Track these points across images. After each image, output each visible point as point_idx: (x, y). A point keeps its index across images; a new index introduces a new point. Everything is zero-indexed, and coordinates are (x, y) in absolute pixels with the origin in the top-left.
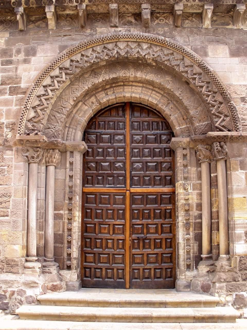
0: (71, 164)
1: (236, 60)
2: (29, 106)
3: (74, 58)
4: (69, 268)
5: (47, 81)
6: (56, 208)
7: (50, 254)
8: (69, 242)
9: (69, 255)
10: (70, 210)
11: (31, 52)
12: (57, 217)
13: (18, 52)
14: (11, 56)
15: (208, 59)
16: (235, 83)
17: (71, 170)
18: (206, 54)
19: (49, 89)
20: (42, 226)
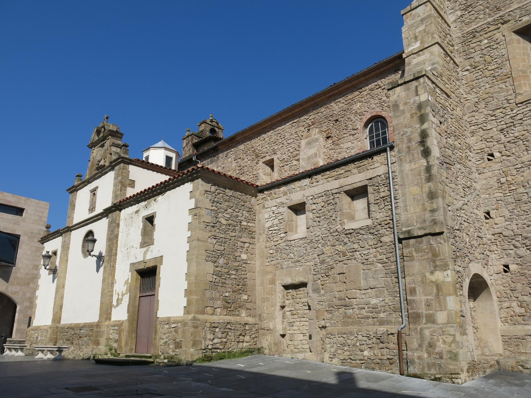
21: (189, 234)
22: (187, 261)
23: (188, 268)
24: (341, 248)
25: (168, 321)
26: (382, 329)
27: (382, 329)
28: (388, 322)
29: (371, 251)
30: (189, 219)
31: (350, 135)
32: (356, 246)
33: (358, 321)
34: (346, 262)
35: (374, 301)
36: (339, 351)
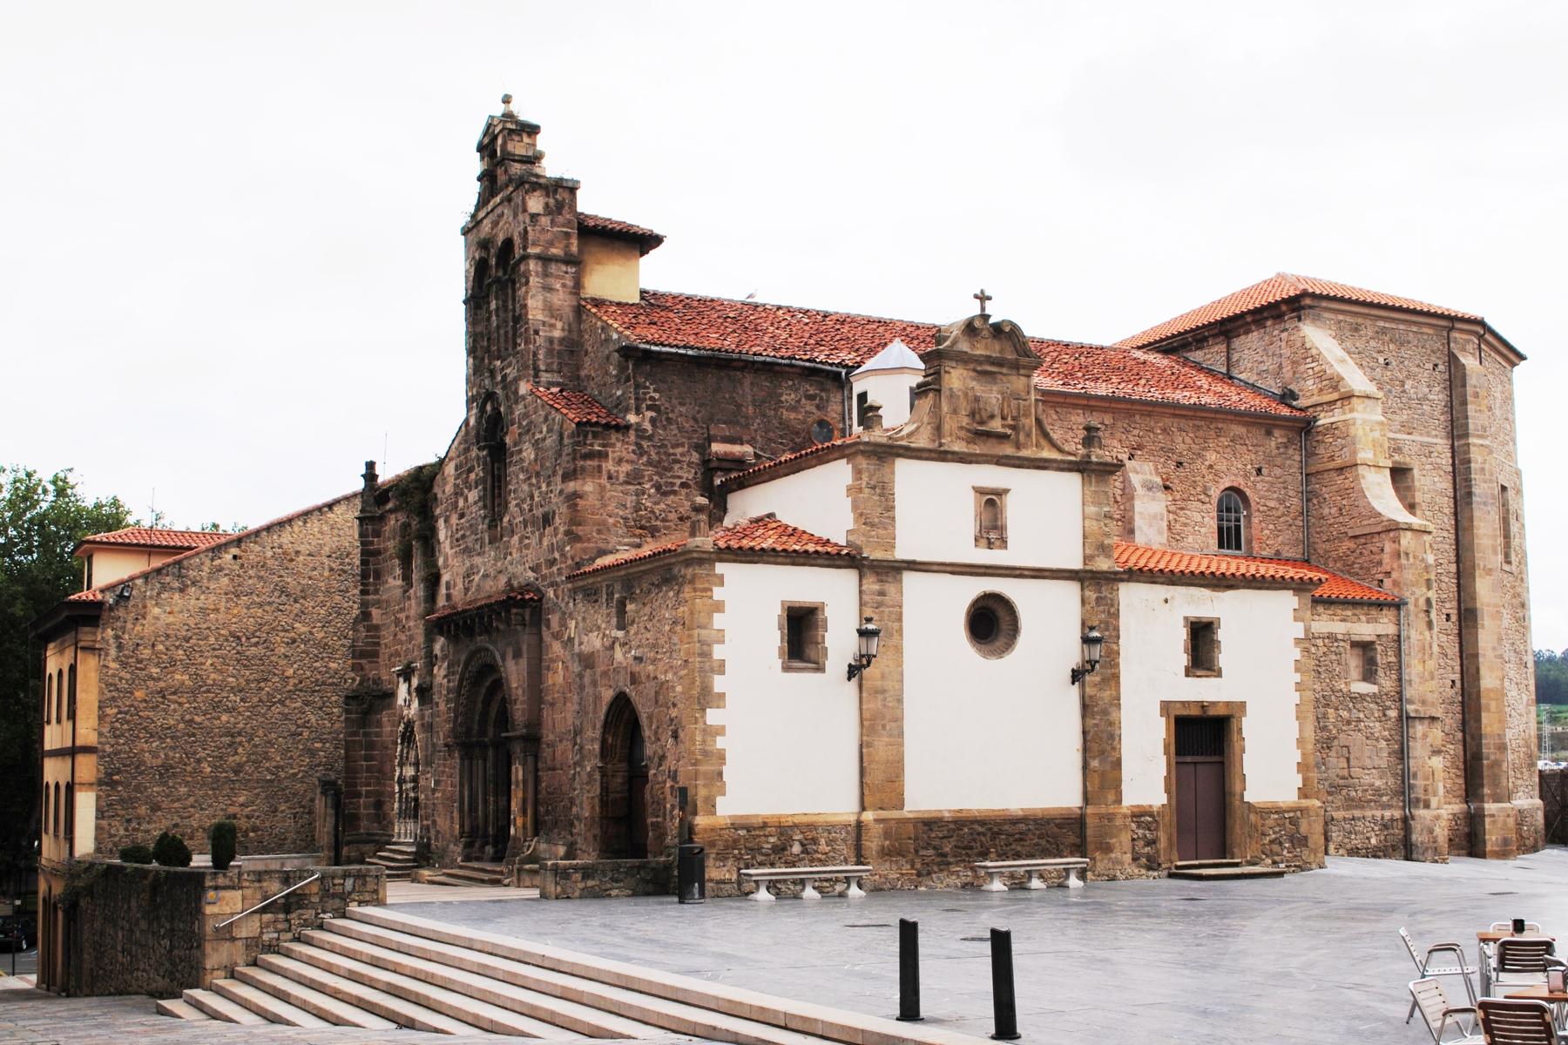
7: (480, 832)
21: (1297, 677)
22: (1298, 718)
23: (1301, 731)
24: (1345, 714)
25: (1264, 812)
26: (1387, 814)
27: (1387, 814)
28: (1390, 807)
29: (1377, 724)
30: (1297, 653)
31: (1199, 500)
32: (1361, 715)
33: (1360, 804)
34: (1350, 733)
35: (1378, 783)
36: (1346, 840)
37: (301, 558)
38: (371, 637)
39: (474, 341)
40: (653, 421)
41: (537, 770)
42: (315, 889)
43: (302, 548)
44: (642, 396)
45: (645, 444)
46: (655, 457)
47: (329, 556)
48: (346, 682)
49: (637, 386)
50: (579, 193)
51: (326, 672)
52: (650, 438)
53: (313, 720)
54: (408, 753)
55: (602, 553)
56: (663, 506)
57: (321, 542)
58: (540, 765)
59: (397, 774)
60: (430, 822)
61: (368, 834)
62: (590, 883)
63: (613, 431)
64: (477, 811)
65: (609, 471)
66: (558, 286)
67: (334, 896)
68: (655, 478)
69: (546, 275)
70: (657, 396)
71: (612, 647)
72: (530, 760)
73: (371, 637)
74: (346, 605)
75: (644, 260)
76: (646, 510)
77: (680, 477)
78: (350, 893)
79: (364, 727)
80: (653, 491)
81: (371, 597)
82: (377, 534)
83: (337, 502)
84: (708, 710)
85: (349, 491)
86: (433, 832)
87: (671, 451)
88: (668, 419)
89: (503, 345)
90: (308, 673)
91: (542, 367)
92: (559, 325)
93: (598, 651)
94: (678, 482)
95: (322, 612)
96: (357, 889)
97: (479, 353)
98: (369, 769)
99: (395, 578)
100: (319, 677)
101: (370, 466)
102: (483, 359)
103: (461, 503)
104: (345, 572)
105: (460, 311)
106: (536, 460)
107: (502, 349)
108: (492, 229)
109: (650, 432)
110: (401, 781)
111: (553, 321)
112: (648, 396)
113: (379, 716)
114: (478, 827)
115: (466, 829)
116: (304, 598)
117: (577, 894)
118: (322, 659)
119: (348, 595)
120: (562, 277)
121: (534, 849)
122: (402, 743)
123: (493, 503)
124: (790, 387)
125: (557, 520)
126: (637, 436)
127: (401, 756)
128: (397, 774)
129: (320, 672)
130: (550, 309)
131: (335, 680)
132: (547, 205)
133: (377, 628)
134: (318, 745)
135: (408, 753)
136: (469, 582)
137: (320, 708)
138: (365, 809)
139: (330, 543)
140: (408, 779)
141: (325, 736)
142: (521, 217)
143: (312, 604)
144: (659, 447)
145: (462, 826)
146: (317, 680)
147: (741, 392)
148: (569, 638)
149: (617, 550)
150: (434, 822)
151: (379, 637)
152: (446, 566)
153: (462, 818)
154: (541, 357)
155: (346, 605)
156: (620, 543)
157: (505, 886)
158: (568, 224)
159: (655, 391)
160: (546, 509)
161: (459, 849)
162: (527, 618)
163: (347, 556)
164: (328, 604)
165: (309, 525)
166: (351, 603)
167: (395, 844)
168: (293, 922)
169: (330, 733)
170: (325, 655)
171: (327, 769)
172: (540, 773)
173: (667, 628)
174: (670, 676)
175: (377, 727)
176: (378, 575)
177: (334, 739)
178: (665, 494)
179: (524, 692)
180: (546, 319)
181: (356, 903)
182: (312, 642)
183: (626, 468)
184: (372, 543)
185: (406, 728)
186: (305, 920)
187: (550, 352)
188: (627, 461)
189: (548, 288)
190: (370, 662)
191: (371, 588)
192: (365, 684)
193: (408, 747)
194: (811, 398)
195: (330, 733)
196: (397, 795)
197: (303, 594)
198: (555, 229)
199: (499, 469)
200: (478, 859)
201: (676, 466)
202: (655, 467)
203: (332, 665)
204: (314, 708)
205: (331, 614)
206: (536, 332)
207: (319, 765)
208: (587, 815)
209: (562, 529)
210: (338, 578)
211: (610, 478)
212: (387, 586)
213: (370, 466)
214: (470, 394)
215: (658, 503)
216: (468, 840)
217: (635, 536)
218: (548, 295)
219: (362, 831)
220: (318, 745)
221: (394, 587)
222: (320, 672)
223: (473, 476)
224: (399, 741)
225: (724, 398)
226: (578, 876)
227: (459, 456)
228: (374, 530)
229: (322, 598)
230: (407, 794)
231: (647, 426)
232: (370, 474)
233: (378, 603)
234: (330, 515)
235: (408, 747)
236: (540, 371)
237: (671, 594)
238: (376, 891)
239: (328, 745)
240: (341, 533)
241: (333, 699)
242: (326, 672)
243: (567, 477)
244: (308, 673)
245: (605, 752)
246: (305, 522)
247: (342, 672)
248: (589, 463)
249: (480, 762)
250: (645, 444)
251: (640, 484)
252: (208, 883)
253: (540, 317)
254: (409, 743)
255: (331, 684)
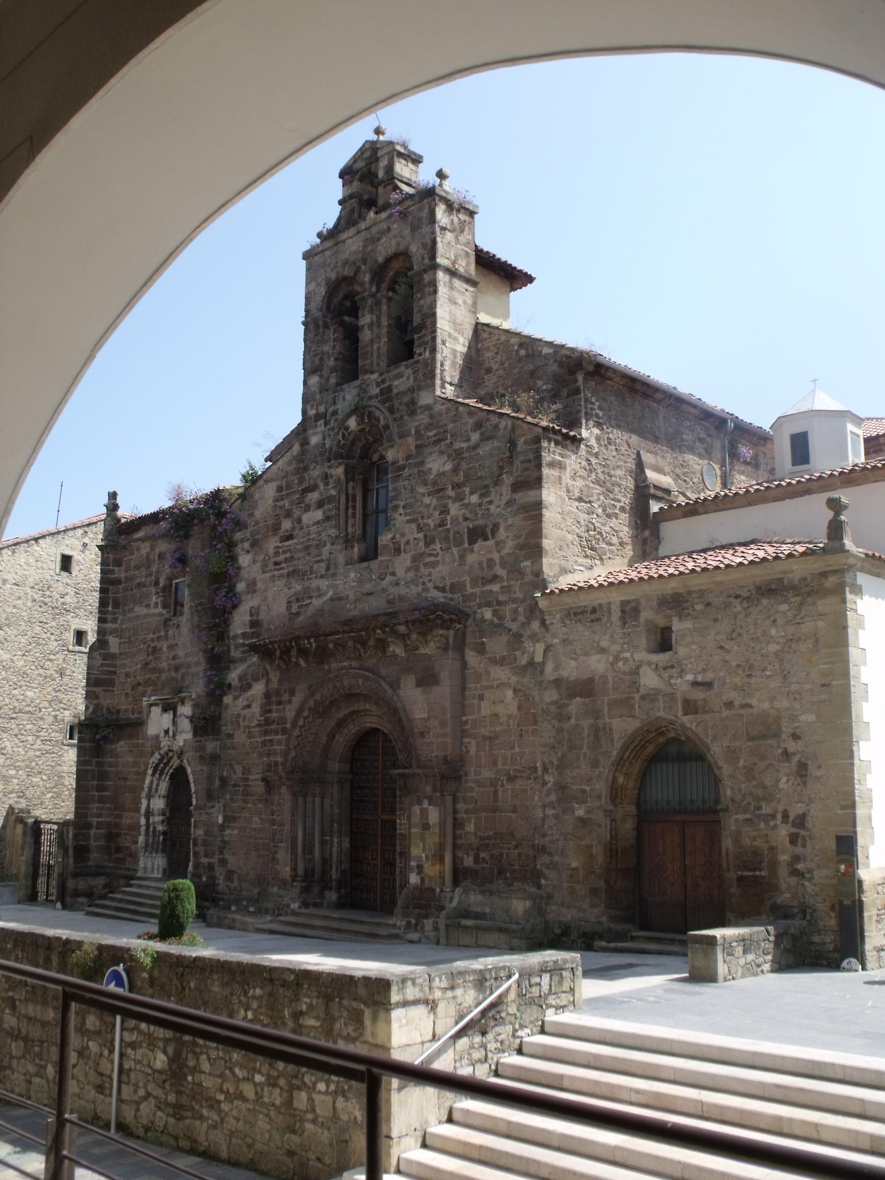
0: (332, 793)
1: (420, 689)
2: (291, 746)
3: (316, 698)
4: (331, 889)
5: (301, 723)
6: (323, 834)
8: (331, 865)
9: (331, 876)
10: (331, 836)
11: (292, 693)
12: (323, 842)
13: (285, 692)
14: (281, 696)
15: (400, 691)
16: (417, 716)
17: (332, 800)
18: (399, 687)
19: (303, 729)
20: (308, 849)
37: (8, 586)
38: (108, 665)
39: (322, 359)
40: (598, 439)
41: (455, 812)
42: (512, 995)
43: (9, 577)
44: (589, 411)
45: (594, 461)
46: (601, 476)
47: (32, 588)
48: (40, 710)
49: (586, 400)
50: (476, 216)
51: (23, 700)
52: (596, 455)
53: (9, 748)
54: (158, 785)
55: (564, 571)
56: (608, 529)
57: (26, 573)
58: (461, 806)
59: (144, 806)
60: (214, 860)
61: (97, 867)
62: (750, 957)
63: (568, 442)
64: (311, 852)
65: (567, 484)
66: (460, 301)
67: (532, 1002)
68: (602, 497)
69: (452, 288)
70: (601, 414)
71: (636, 672)
72: (449, 799)
73: (108, 665)
74: (44, 636)
75: (513, 294)
76: (595, 530)
77: (619, 501)
78: (546, 996)
79: (98, 757)
80: (600, 511)
81: (109, 626)
82: (118, 563)
83: (43, 537)
84: (861, 742)
85: (85, 518)
86: (220, 873)
87: (612, 472)
88: (609, 439)
89: (375, 360)
90: (7, 701)
91: (448, 379)
92: (461, 340)
93: (604, 677)
94: (618, 505)
95: (23, 640)
96: (553, 991)
97: (325, 372)
98: (101, 800)
99: (148, 606)
100: (16, 704)
101: (113, 496)
102: (328, 379)
103: (287, 525)
104: (46, 604)
105: (299, 331)
106: (455, 470)
107: (375, 364)
108: (364, 247)
109: (597, 450)
110: (148, 813)
111: (456, 335)
112: (594, 413)
113: (113, 746)
114: (313, 869)
115: (300, 872)
116: (8, 626)
117: (739, 973)
118: (20, 687)
119: (46, 626)
120: (463, 293)
121: (459, 902)
122: (153, 775)
123: (347, 523)
124: (687, 427)
125: (502, 533)
126: (587, 452)
127: (150, 788)
128: (144, 806)
129: (17, 700)
130: (454, 322)
131: (31, 709)
132: (452, 221)
133: (113, 656)
134: (12, 772)
135: (158, 785)
136: (299, 607)
137: (16, 736)
138: (95, 841)
139: (34, 576)
140: (156, 812)
141: (18, 764)
142: (426, 229)
143: (15, 632)
144: (604, 466)
145: (294, 869)
146: (15, 707)
147: (657, 424)
148: (531, 663)
149: (575, 570)
150: (223, 862)
151: (115, 666)
152: (252, 588)
153: (294, 859)
154: (447, 368)
155: (44, 636)
156: (576, 562)
157: (411, 942)
158: (467, 244)
159: (600, 408)
160: (480, 522)
161: (295, 892)
162: (451, 640)
163: (48, 588)
164: (29, 633)
165: (17, 555)
166: (49, 635)
167: (140, 879)
168: (489, 1046)
169: (23, 761)
170: (23, 683)
171: (19, 797)
172: (459, 816)
173: (773, 648)
174: (783, 703)
175: (111, 757)
176: (116, 605)
177: (27, 767)
178: (609, 516)
179: (443, 724)
180: (452, 332)
181: (552, 1010)
182: (12, 670)
183: (580, 483)
184: (113, 572)
185: (161, 760)
186: (502, 1042)
187: (454, 363)
188: (580, 476)
189: (453, 301)
190: (105, 691)
191: (109, 617)
192: (99, 713)
193: (159, 779)
194: (701, 440)
195: (23, 761)
196: (143, 829)
197: (7, 622)
198: (458, 246)
199: (353, 488)
200: (316, 905)
201: (617, 489)
202: (601, 486)
203: (29, 694)
204: (11, 734)
205: (31, 644)
206: (444, 343)
207: (11, 792)
208: (574, 864)
209: (510, 544)
210: (39, 609)
211: (568, 491)
212: (132, 615)
213: (113, 496)
214: (312, 412)
215: (604, 525)
216: (304, 884)
217: (586, 557)
218: (453, 307)
219: (91, 863)
220: (12, 772)
221: (146, 616)
222: (17, 700)
223: (314, 496)
224: (150, 772)
225: (646, 427)
226: (740, 949)
227: (286, 476)
228: (114, 560)
229: (24, 628)
230: (155, 828)
231: (593, 442)
232: (112, 507)
233: (113, 632)
234: (36, 548)
235: (159, 779)
236: (445, 382)
237: (784, 607)
238: (572, 990)
239: (21, 772)
240: (45, 566)
241: (28, 727)
242: (23, 700)
243: (516, 487)
244: (7, 701)
245: (615, 793)
246: (14, 552)
247: (38, 701)
248: (552, 472)
249: (317, 800)
250: (594, 461)
251: (590, 502)
252: (395, 997)
253: (446, 328)
254: (161, 775)
255: (26, 713)
